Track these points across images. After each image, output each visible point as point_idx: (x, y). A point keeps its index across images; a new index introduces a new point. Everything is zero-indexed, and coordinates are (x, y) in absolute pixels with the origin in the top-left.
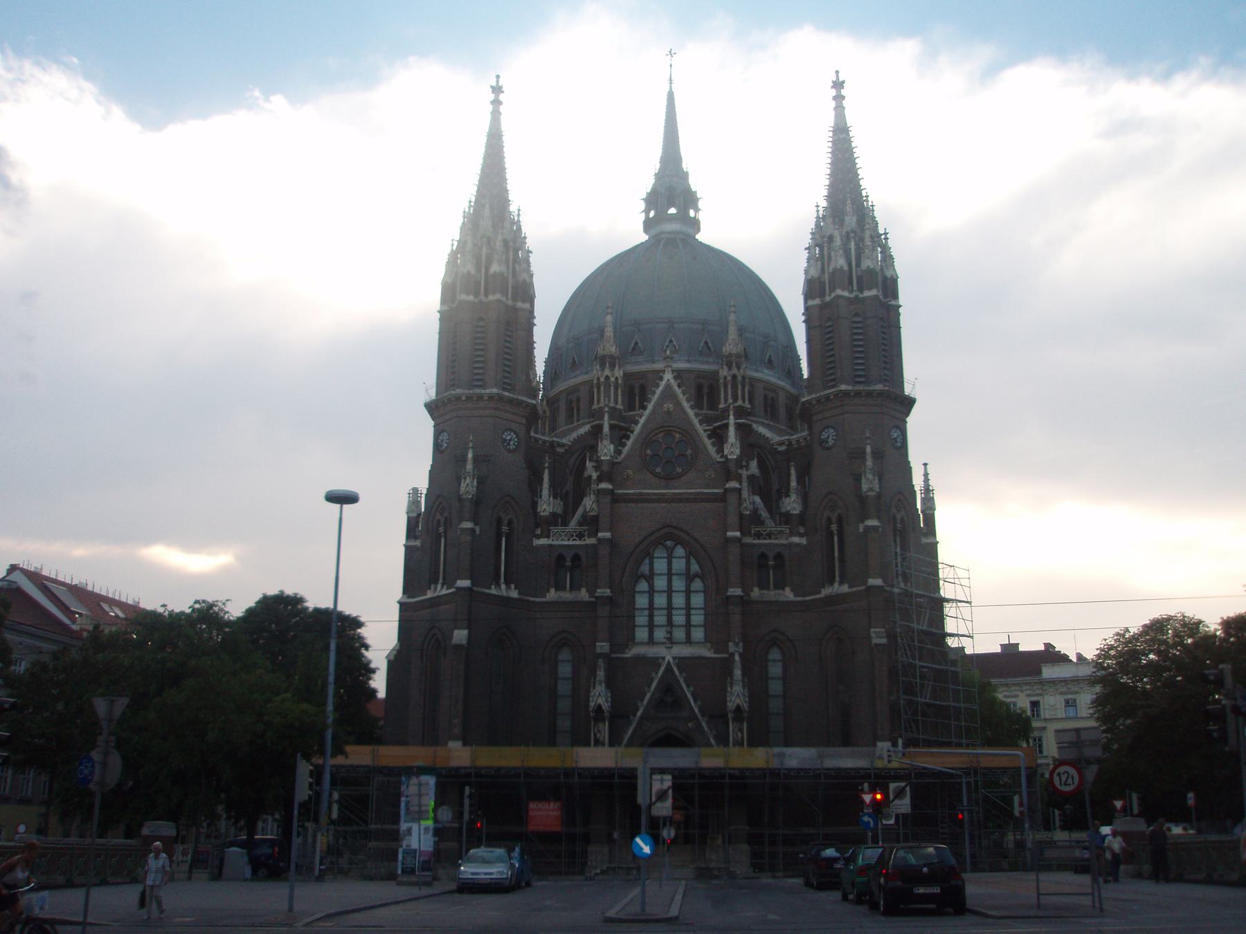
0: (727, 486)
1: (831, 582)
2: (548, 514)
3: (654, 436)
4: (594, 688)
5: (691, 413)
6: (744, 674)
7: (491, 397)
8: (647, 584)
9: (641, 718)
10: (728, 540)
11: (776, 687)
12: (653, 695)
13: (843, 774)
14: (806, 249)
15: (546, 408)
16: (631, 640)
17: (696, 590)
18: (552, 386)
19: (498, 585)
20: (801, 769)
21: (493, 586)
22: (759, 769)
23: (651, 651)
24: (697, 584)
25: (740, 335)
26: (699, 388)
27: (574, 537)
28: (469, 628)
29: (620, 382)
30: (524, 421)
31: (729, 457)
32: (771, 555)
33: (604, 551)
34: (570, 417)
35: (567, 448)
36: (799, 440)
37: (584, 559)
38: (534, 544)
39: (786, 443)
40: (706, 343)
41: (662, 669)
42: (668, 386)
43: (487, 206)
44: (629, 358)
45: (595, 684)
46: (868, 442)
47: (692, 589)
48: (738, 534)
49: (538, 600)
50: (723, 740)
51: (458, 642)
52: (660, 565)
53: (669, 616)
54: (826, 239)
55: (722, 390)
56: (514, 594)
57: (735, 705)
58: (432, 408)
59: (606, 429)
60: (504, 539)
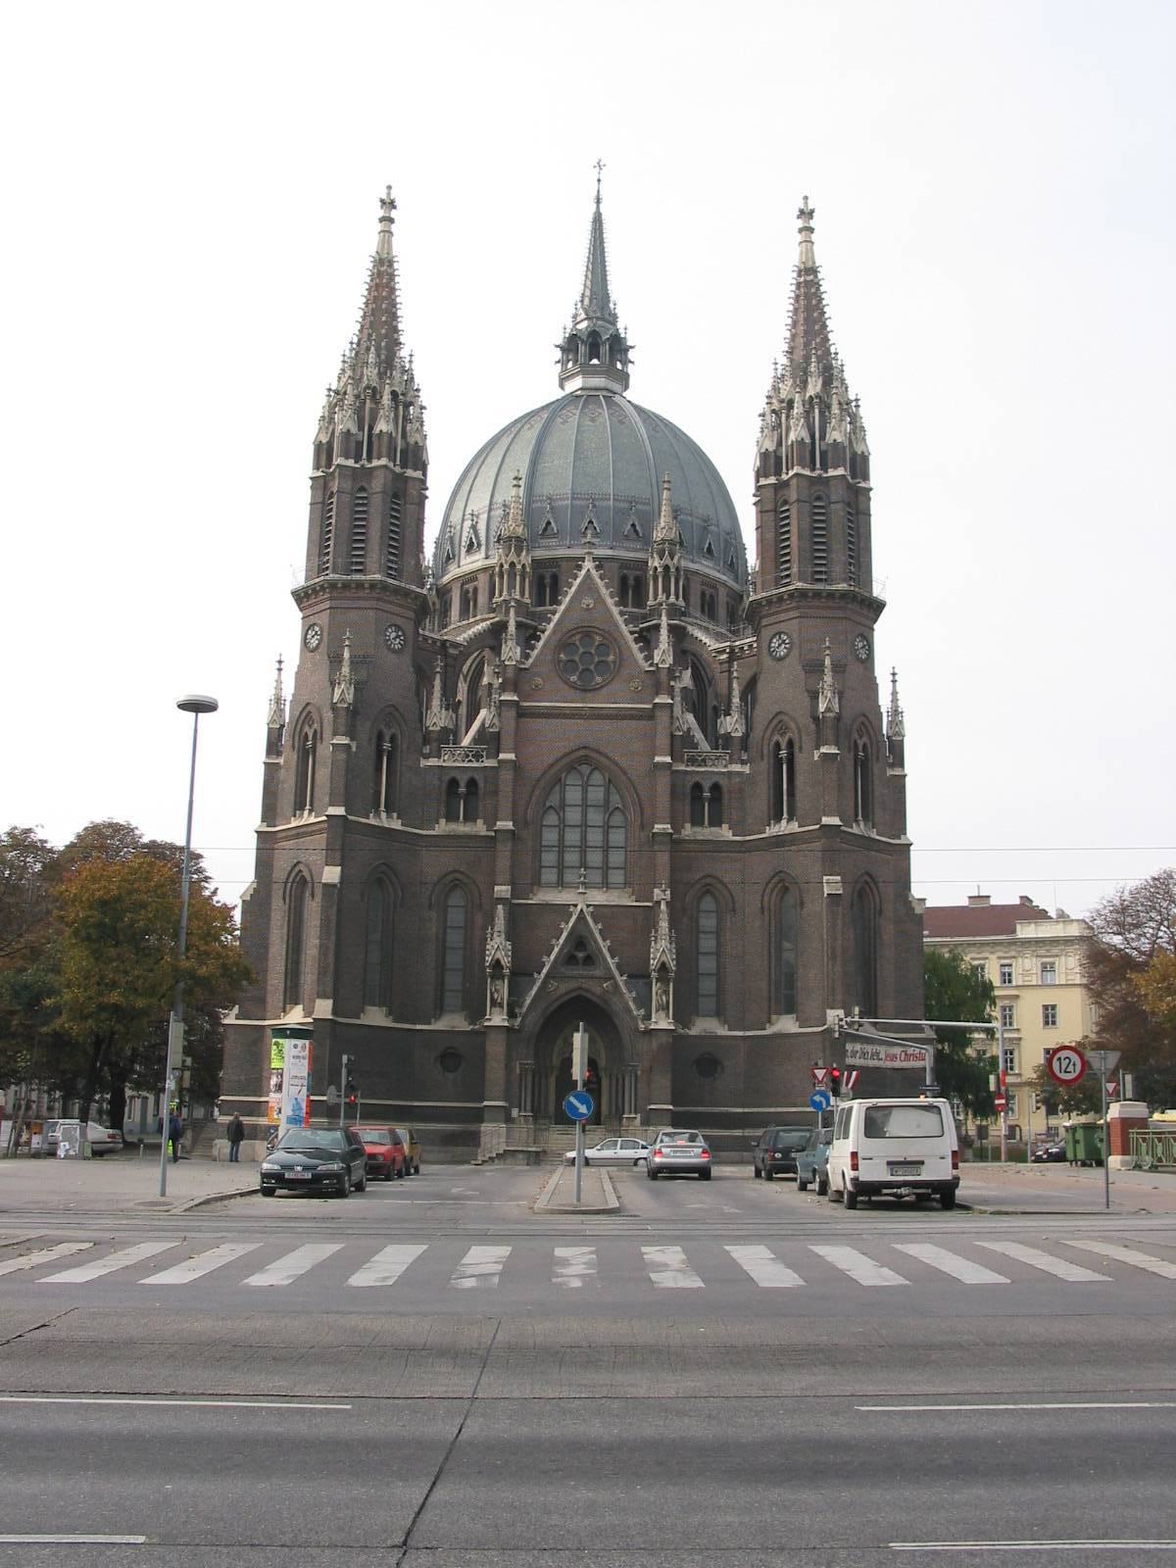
0: (657, 701)
1: (778, 818)
3: (570, 638)
5: (615, 610)
7: (373, 585)
8: (556, 817)
9: (547, 976)
10: (657, 765)
12: (561, 950)
14: (760, 416)
15: (436, 600)
19: (378, 814)
24: (617, 819)
25: (675, 518)
26: (624, 580)
29: (528, 570)
30: (412, 615)
32: (707, 785)
33: (507, 776)
34: (465, 612)
37: (481, 784)
38: (422, 766)
39: (728, 651)
40: (633, 525)
43: (373, 348)
45: (492, 935)
48: (668, 759)
52: (573, 795)
54: (784, 405)
55: (651, 583)
58: (301, 597)
59: (512, 628)
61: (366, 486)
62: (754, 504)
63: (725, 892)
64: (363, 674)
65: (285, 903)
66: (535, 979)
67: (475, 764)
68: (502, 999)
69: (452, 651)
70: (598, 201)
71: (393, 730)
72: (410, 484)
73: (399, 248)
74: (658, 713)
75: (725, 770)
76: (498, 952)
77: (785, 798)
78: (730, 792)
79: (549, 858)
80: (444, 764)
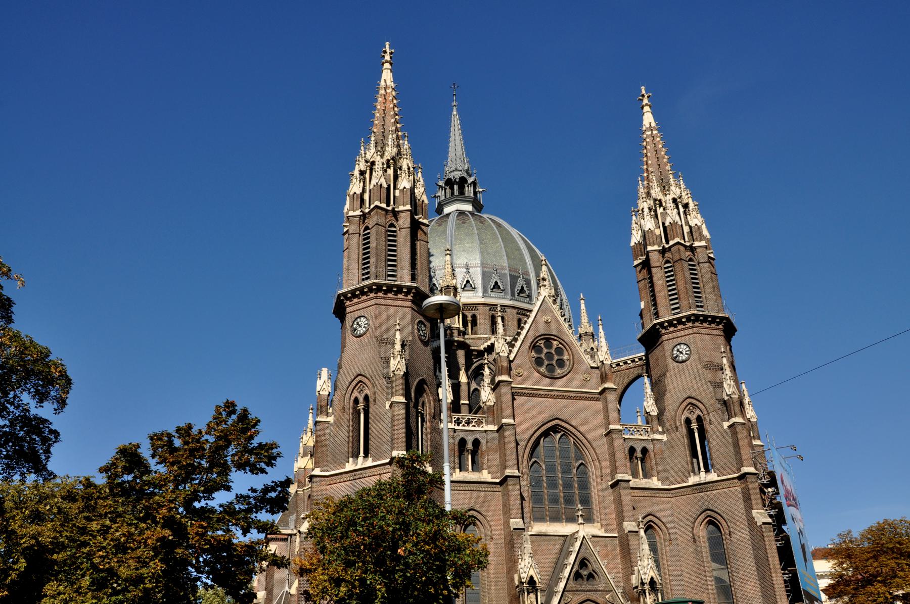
27: (473, 424)
32: (639, 449)
37: (483, 444)
57: (650, 578)
67: (477, 428)
76: (531, 569)
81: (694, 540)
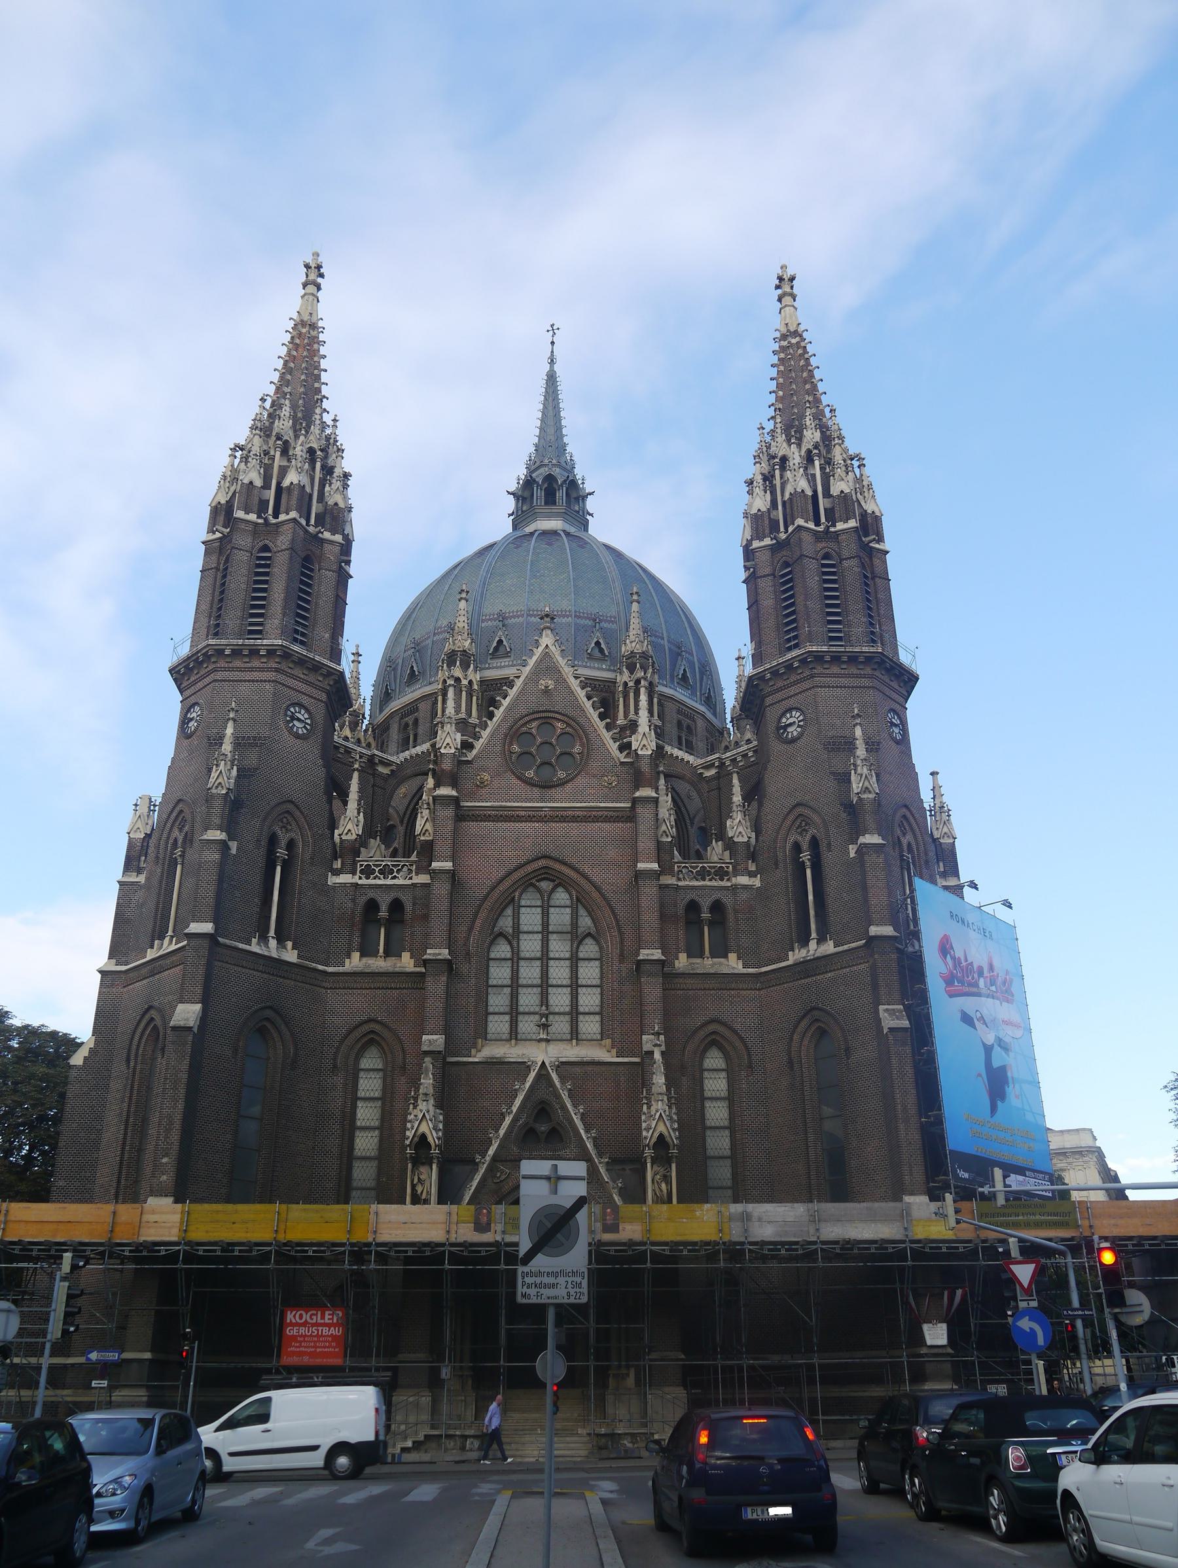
0: (637, 794)
1: (805, 942)
2: (354, 837)
4: (415, 1107)
6: (669, 1083)
7: (271, 652)
8: (508, 948)
9: (495, 1159)
10: (638, 875)
11: (717, 1113)
12: (514, 1120)
13: (856, 1251)
15: (371, 740)
16: (482, 1033)
17: (586, 956)
18: (381, 711)
19: (264, 938)
20: (783, 1243)
21: (254, 941)
22: (708, 1243)
23: (512, 1052)
24: (589, 948)
28: (205, 1001)
29: (476, 687)
30: (324, 697)
31: (640, 752)
32: (705, 903)
33: (442, 889)
35: (394, 768)
36: (736, 759)
37: (408, 907)
40: (598, 644)
41: (532, 1075)
42: (546, 655)
44: (489, 661)
46: (858, 721)
47: (581, 955)
49: (330, 969)
50: (634, 1195)
51: (182, 1023)
52: (530, 918)
53: (544, 1000)
56: (291, 955)
57: (656, 1135)
60: (279, 869)
61: (270, 545)
62: (743, 582)
63: (738, 1044)
64: (252, 760)
65: (128, 1068)
66: (477, 1164)
68: (429, 1193)
69: (381, 769)
70: (552, 362)
71: (292, 835)
72: (327, 547)
73: (329, 312)
74: (639, 810)
75: (729, 884)
76: (424, 1123)
77: (812, 912)
78: (736, 911)
79: (498, 1001)
80: (360, 882)
81: (791, 1067)
